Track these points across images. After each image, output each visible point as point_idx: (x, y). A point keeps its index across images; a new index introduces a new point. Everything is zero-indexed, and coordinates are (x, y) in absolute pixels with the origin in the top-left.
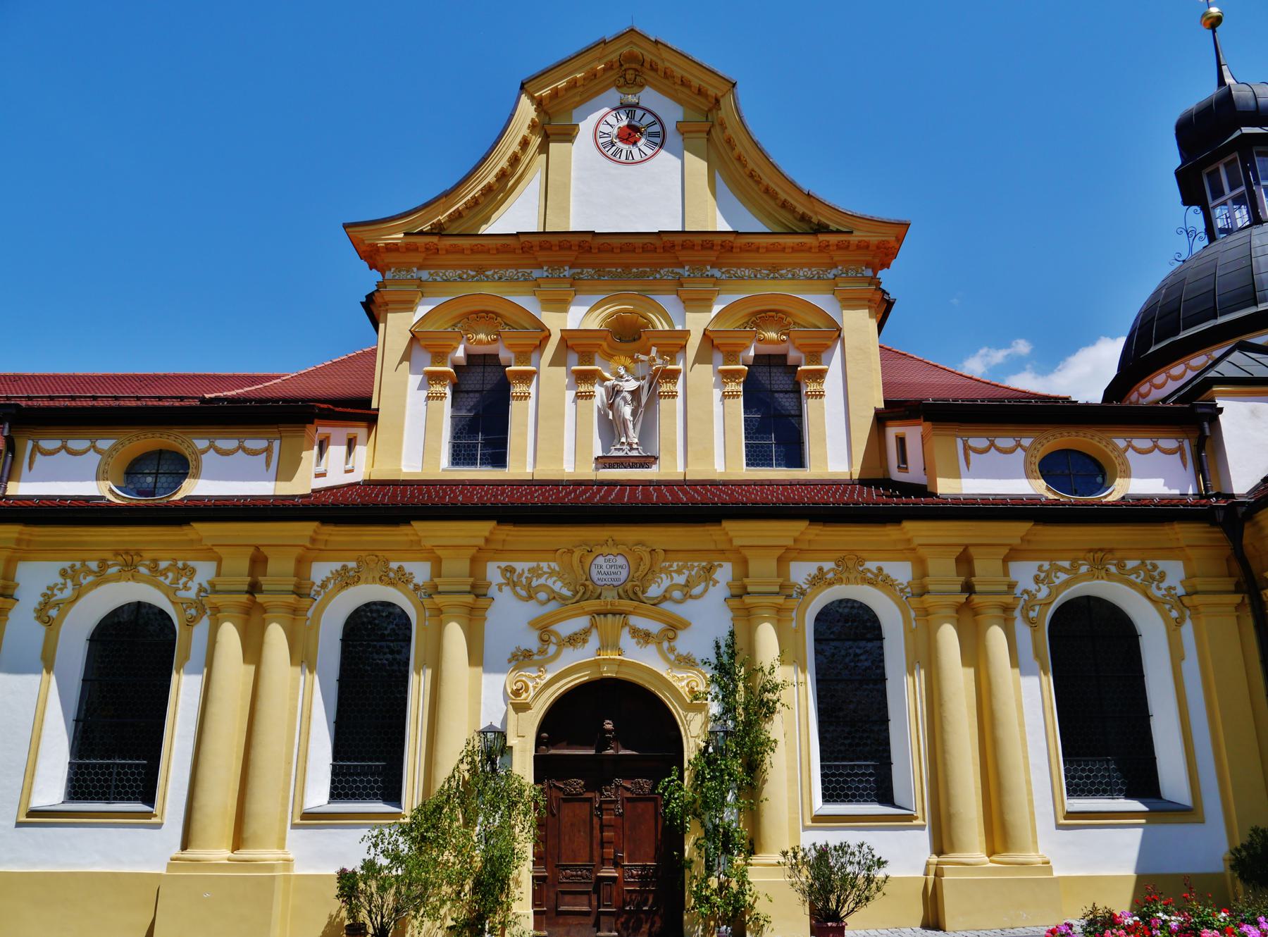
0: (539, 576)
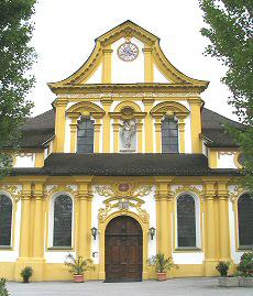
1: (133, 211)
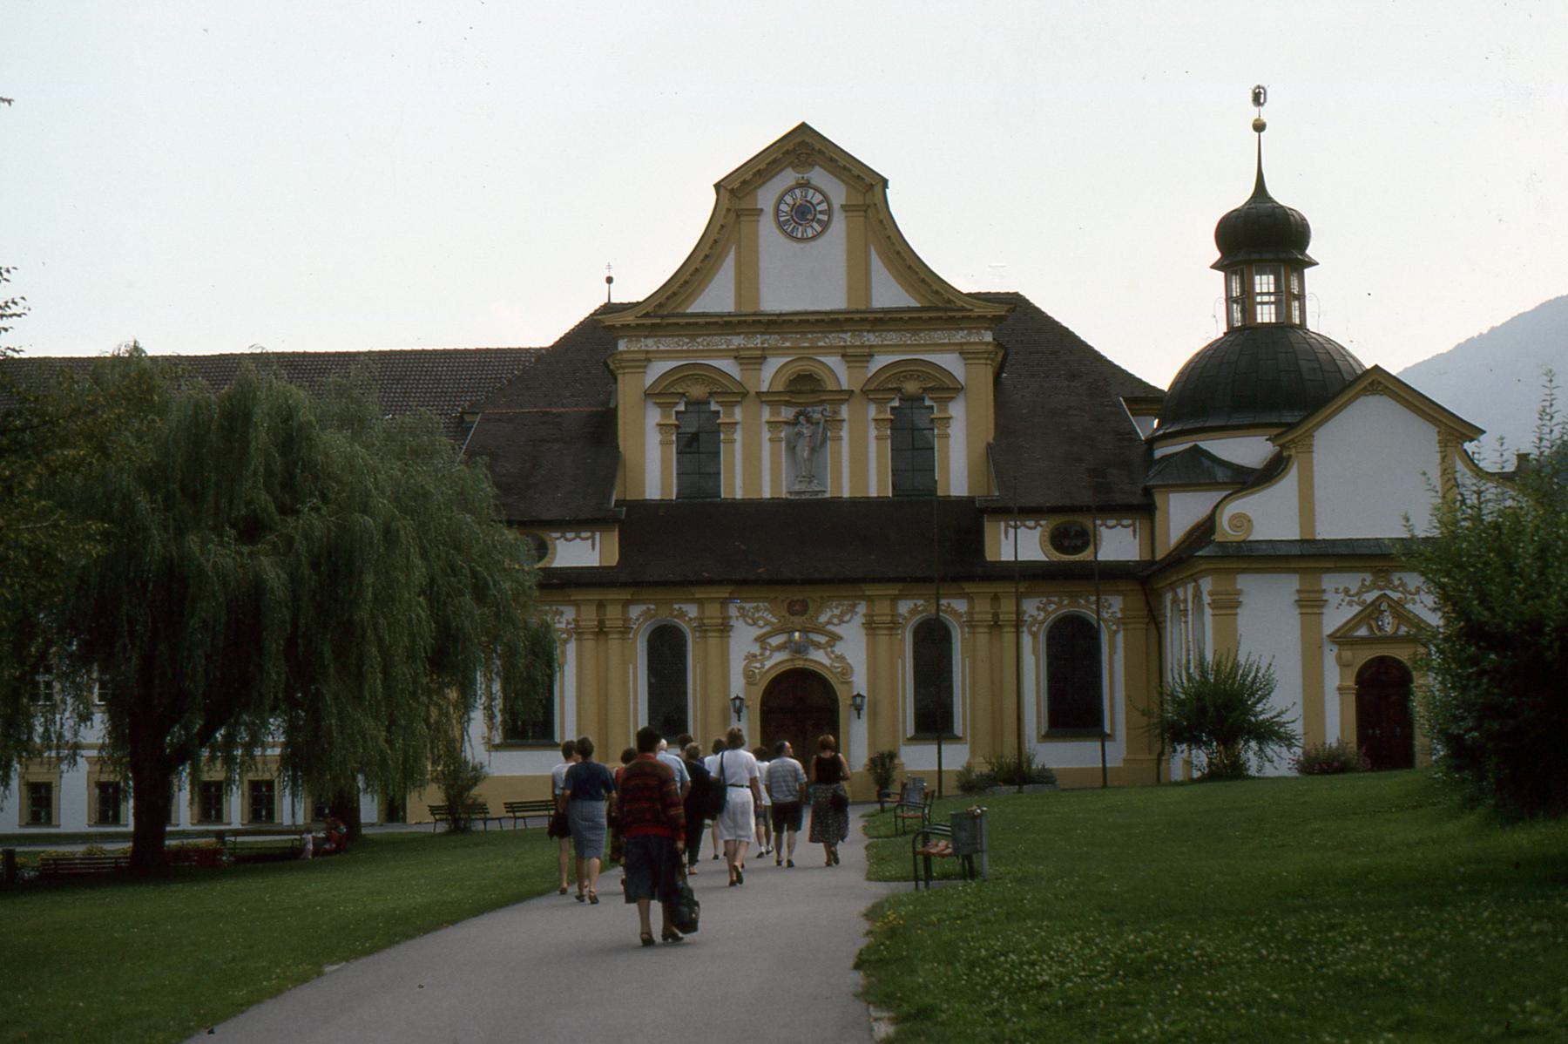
0: (759, 611)
1: (819, 657)
